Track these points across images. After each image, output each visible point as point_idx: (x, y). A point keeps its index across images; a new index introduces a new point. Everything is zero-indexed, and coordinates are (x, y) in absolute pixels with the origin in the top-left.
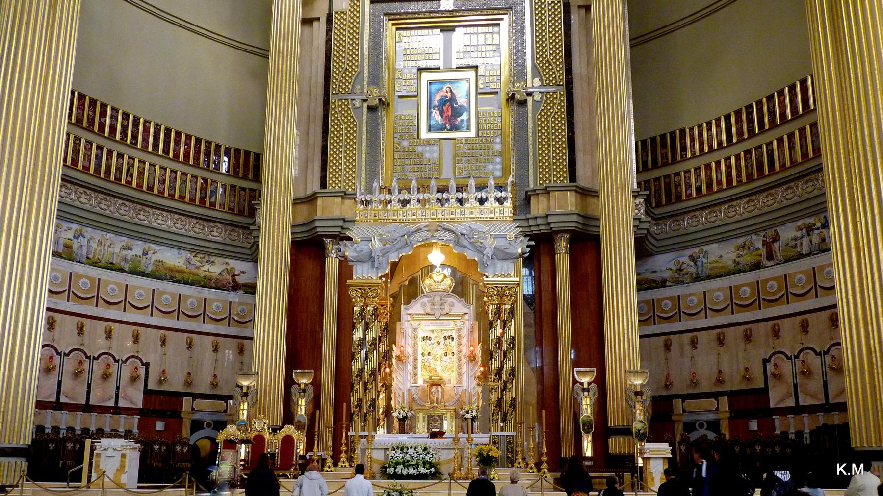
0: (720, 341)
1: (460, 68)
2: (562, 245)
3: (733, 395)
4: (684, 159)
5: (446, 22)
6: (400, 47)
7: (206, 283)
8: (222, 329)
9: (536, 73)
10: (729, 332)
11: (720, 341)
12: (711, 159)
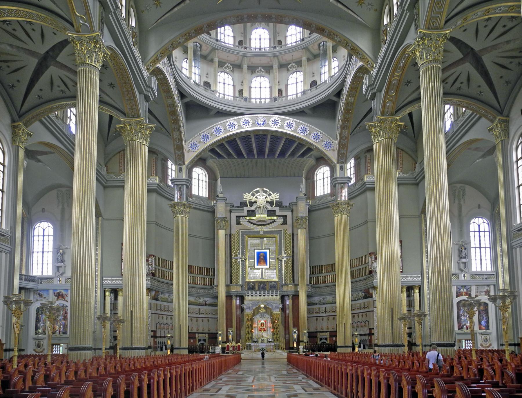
0: (328, 319)
1: (265, 249)
2: (291, 297)
3: (330, 332)
4: (322, 273)
5: (262, 236)
6: (249, 243)
7: (199, 304)
8: (203, 316)
9: (285, 253)
10: (330, 317)
11: (328, 319)
12: (328, 274)
